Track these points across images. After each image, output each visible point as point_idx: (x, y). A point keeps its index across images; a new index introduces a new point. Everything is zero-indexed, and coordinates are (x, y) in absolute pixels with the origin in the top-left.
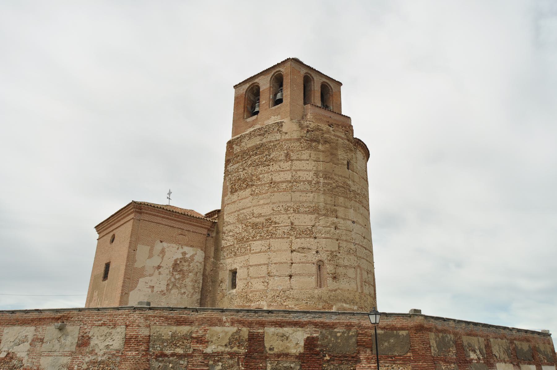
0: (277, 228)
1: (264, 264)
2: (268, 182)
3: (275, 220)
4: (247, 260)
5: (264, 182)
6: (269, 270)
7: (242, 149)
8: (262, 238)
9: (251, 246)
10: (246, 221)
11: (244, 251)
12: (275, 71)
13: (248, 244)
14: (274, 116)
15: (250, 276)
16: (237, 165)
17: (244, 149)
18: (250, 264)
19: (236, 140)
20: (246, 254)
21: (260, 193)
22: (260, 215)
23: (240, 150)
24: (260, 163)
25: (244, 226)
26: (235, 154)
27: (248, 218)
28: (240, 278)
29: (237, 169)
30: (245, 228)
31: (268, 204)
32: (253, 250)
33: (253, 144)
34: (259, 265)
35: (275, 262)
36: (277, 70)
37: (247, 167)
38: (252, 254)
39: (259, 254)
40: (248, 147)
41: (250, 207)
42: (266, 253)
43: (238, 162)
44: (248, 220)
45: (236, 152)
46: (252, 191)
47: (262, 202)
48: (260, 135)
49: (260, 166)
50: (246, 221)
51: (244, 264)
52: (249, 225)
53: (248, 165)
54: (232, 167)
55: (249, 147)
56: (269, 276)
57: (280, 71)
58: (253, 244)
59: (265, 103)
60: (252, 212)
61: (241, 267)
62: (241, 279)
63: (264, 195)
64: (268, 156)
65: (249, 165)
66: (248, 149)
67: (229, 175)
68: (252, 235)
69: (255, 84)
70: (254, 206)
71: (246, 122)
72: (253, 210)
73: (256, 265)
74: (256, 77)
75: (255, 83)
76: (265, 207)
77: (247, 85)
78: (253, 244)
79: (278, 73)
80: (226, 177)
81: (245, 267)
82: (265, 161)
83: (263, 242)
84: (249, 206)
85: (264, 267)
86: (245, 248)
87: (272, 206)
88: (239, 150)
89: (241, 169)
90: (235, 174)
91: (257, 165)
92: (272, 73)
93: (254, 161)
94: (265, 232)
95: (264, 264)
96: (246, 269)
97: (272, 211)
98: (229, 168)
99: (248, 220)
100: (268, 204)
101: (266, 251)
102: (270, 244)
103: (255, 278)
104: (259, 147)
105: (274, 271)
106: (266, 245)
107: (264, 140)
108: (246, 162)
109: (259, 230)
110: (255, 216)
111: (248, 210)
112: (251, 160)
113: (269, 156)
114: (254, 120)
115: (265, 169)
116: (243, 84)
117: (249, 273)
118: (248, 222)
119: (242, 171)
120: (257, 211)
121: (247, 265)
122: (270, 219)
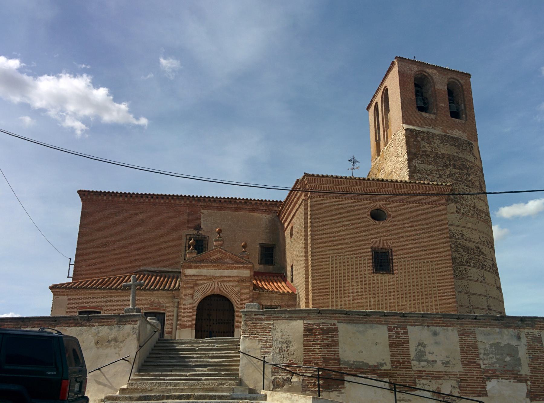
0: (485, 259)
1: (484, 296)
2: (472, 205)
3: (482, 250)
4: (466, 285)
5: (469, 204)
6: (489, 303)
7: (434, 150)
8: (475, 266)
9: (467, 272)
10: (456, 240)
11: (460, 274)
12: (453, 76)
13: (464, 268)
14: (459, 130)
15: (472, 304)
16: (430, 167)
17: (437, 152)
18: (471, 291)
19: (421, 133)
20: (464, 279)
21: (467, 214)
22: (469, 240)
23: (431, 150)
24: (460, 180)
25: (453, 246)
26: (423, 151)
27: (457, 237)
28: (460, 304)
29: (429, 172)
30: (454, 248)
31: (475, 230)
32: (471, 277)
33: (449, 153)
34: (480, 295)
35: (491, 295)
36: (455, 77)
37: (445, 176)
38: (471, 280)
39: (477, 283)
40: (442, 152)
41: (459, 226)
42: (482, 284)
43: (430, 164)
44: (458, 241)
45: (425, 149)
46: (457, 207)
47: (470, 225)
48: (455, 146)
49: (461, 183)
50: (456, 240)
51: (463, 289)
52: (459, 246)
53: (446, 175)
54: (422, 166)
55: (444, 153)
56: (489, 309)
57: (458, 80)
58: (470, 270)
59: (445, 107)
60: (462, 233)
61: (460, 292)
62: (462, 306)
63: (470, 218)
64: (468, 176)
65: (448, 174)
66: (443, 156)
67: (418, 173)
68: (465, 258)
69: (425, 74)
70: (463, 227)
71: (422, 115)
72: (462, 231)
73: (477, 294)
74: (429, 67)
75: (425, 72)
76: (474, 232)
77: (416, 68)
78: (470, 270)
79: (454, 81)
80: (413, 173)
81: (465, 293)
82: (465, 180)
83: (477, 270)
84: (456, 224)
85: (485, 298)
86: (460, 271)
87: (480, 234)
88: (429, 150)
89: (436, 174)
90: (426, 176)
91: (458, 180)
92: (449, 77)
93: (454, 174)
94: (476, 259)
95: (484, 296)
96: (466, 296)
97: (479, 240)
98: (416, 163)
99: (458, 241)
100: (475, 230)
101: (481, 282)
102: (483, 275)
103: (478, 308)
104: (457, 160)
105: (492, 305)
106: (481, 275)
107: (461, 155)
108: (443, 170)
109: (472, 256)
110: (465, 238)
111: (455, 228)
112: (449, 171)
113: (469, 176)
114: (433, 119)
115: (467, 190)
116: (410, 62)
117: (470, 301)
118: (457, 241)
119: (438, 178)
120: (467, 233)
121: (466, 291)
122: (479, 248)
